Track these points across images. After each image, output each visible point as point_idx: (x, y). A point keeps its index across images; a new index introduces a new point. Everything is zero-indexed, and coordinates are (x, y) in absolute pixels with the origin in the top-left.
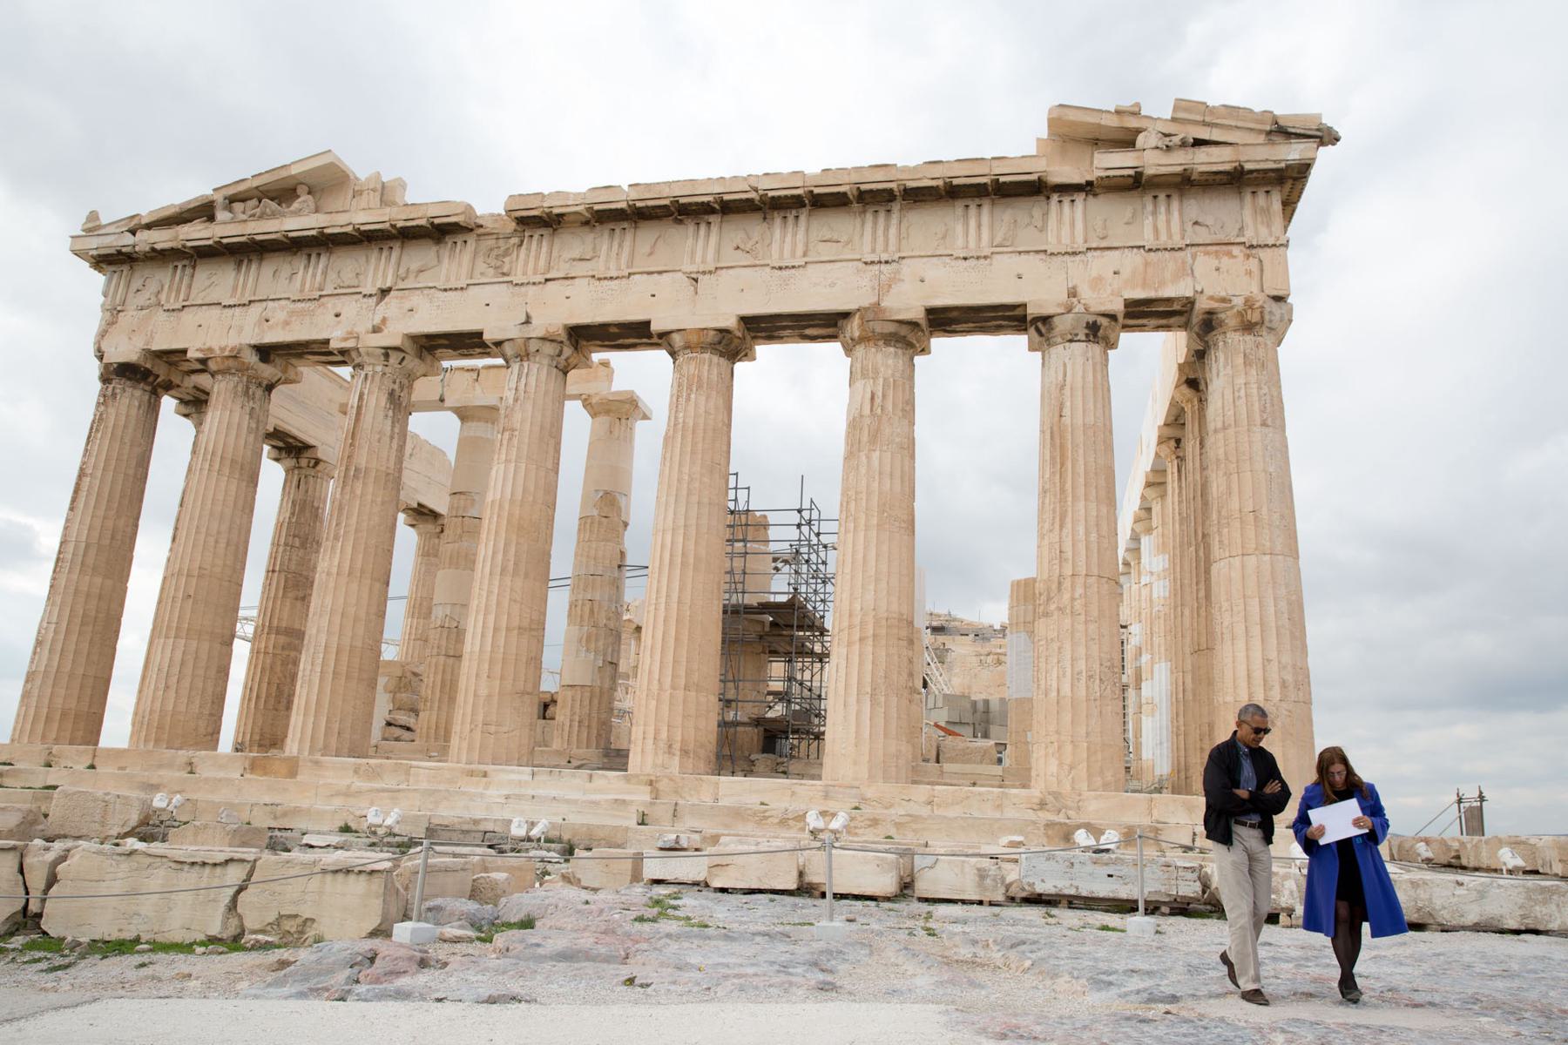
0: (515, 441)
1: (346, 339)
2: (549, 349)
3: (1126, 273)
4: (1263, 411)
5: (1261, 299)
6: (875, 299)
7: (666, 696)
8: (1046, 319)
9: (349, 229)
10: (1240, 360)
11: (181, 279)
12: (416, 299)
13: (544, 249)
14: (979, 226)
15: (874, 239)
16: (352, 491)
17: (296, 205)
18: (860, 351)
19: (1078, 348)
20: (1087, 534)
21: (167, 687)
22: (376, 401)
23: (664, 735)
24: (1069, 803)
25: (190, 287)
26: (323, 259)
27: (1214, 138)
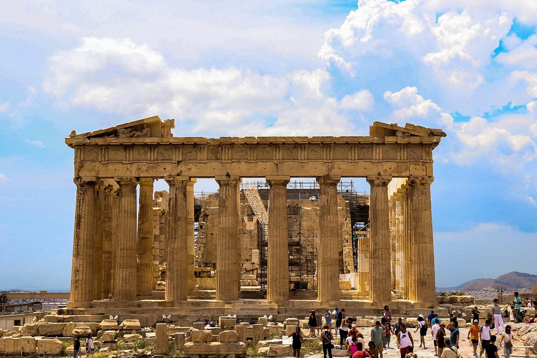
2: (234, 182)
3: (393, 168)
6: (327, 173)
8: (372, 181)
9: (168, 143)
10: (420, 193)
11: (105, 153)
12: (191, 166)
13: (230, 152)
14: (355, 153)
15: (327, 155)
17: (145, 131)
18: (323, 186)
19: (380, 188)
22: (180, 196)
26: (156, 149)
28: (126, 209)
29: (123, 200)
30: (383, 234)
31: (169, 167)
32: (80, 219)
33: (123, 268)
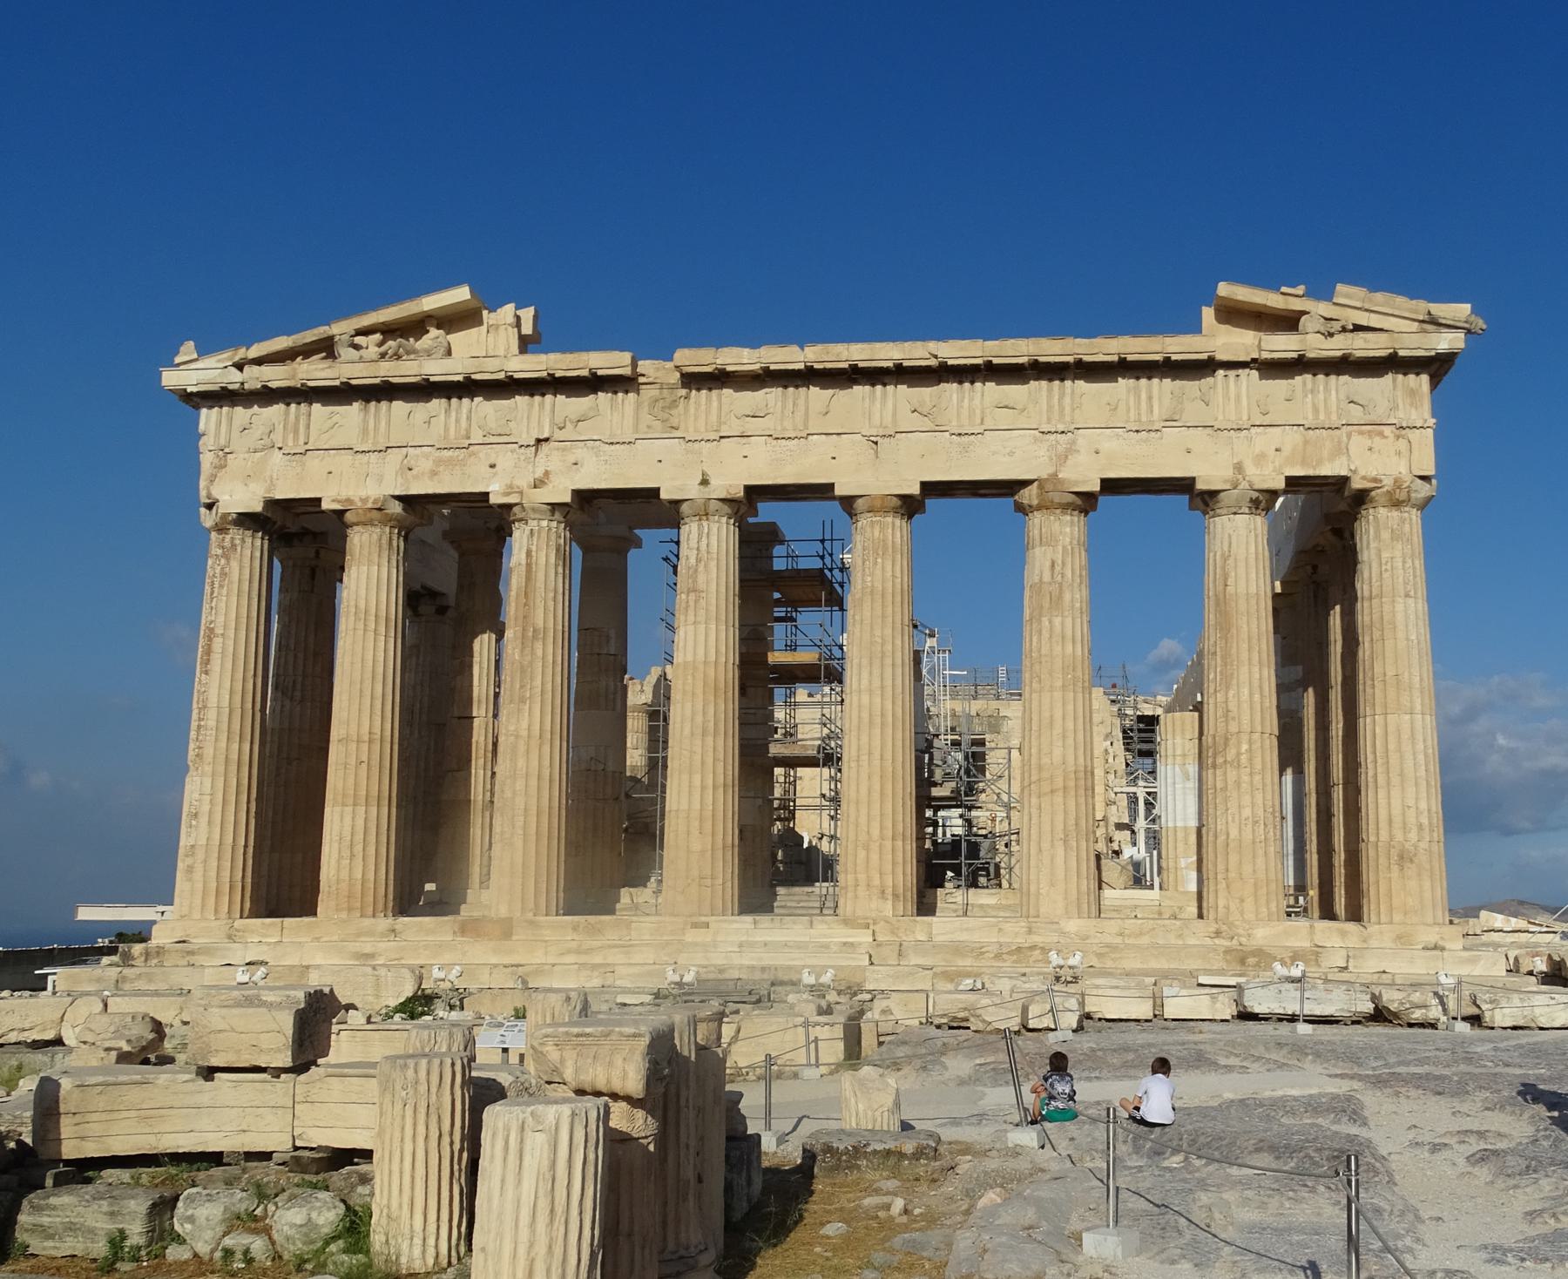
0: (703, 603)
1: (508, 494)
4: (1406, 583)
5: (1407, 479)
6: (1051, 470)
7: (875, 847)
8: (1214, 494)
9: (501, 376)
12: (579, 452)
16: (533, 653)
20: (1251, 695)
21: (352, 856)
23: (877, 882)
24: (1241, 931)
25: (308, 427)
27: (1372, 324)
28: (362, 605)
29: (354, 569)
30: (1256, 683)
31: (506, 459)
32: (210, 640)
33: (344, 805)
